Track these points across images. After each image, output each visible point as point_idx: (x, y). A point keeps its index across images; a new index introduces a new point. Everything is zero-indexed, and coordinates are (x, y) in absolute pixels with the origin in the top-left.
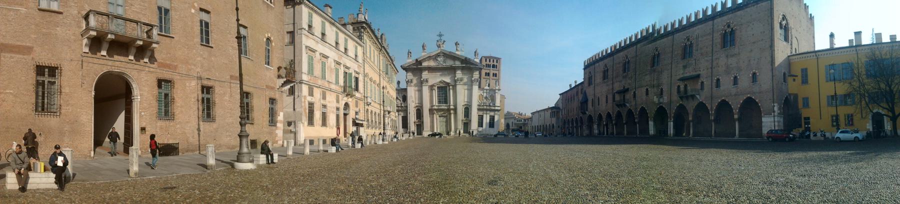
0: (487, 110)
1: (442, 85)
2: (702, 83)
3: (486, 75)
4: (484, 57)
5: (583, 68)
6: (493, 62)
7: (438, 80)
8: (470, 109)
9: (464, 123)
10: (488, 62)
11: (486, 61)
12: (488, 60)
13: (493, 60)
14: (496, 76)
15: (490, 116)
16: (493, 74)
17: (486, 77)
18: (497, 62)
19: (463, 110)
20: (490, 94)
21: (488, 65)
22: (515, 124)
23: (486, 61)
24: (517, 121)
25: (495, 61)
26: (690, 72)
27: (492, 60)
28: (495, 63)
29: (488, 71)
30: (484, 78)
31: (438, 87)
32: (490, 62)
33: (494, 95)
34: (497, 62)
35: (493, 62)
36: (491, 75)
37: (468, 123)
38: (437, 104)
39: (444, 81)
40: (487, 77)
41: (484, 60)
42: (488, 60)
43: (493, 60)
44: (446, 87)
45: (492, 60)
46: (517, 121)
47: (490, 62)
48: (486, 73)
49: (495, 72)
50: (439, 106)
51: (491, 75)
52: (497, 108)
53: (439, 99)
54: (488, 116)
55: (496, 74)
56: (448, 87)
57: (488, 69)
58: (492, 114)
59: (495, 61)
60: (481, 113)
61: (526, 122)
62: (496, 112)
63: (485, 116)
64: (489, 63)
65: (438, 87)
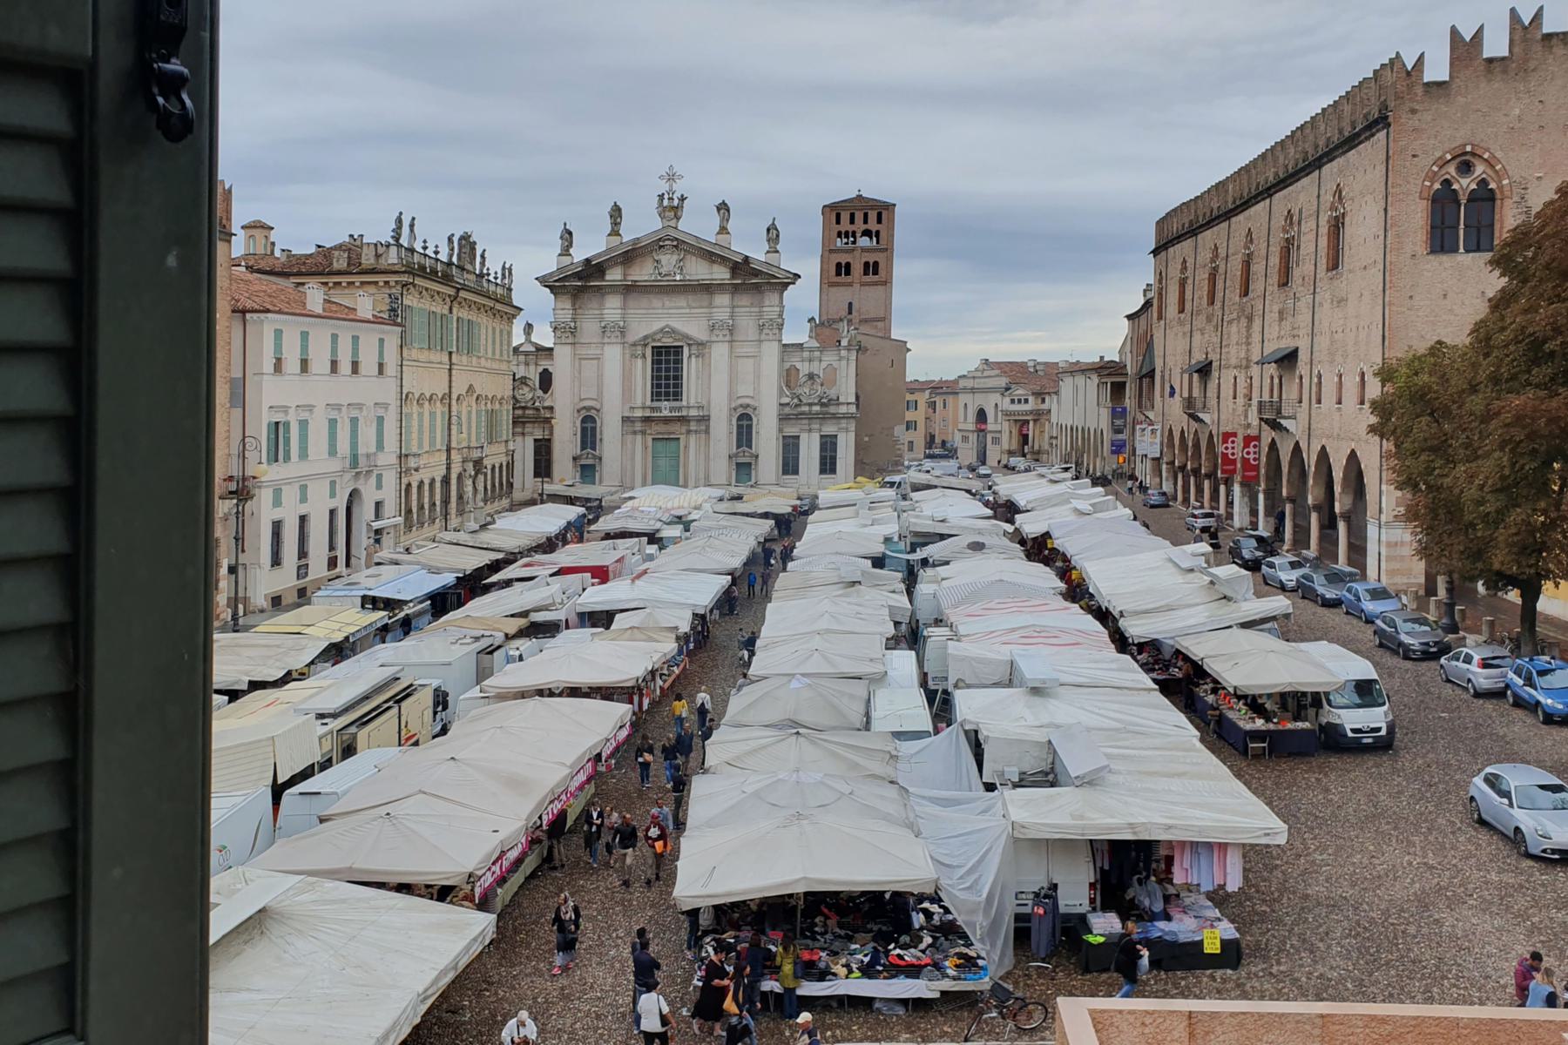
0: (811, 417)
1: (668, 341)
2: (1301, 377)
3: (838, 274)
5: (1153, 247)
6: (866, 222)
7: (657, 326)
8: (755, 419)
9: (737, 464)
10: (845, 225)
11: (838, 222)
12: (845, 217)
13: (866, 215)
14: (876, 272)
15: (822, 436)
16: (867, 264)
17: (838, 279)
18: (879, 221)
19: (734, 422)
20: (824, 365)
22: (1007, 414)
23: (838, 222)
24: (1013, 401)
25: (873, 216)
26: (1287, 344)
27: (859, 216)
28: (873, 225)
29: (844, 259)
31: (653, 347)
32: (852, 221)
33: (835, 364)
34: (879, 221)
35: (866, 222)
36: (857, 269)
37: (750, 464)
38: (648, 403)
39: (674, 331)
40: (843, 278)
42: (845, 217)
43: (866, 215)
44: (682, 347)
45: (859, 216)
46: (1013, 401)
47: (852, 221)
48: (839, 265)
49: (871, 258)
50: (653, 409)
51: (857, 269)
52: (843, 409)
54: (816, 438)
55: (876, 264)
56: (686, 350)
57: (847, 251)
58: (829, 429)
59: (873, 216)
60: (791, 430)
61: (1045, 406)
62: (844, 423)
63: (804, 437)
64: (850, 228)
65: (653, 347)
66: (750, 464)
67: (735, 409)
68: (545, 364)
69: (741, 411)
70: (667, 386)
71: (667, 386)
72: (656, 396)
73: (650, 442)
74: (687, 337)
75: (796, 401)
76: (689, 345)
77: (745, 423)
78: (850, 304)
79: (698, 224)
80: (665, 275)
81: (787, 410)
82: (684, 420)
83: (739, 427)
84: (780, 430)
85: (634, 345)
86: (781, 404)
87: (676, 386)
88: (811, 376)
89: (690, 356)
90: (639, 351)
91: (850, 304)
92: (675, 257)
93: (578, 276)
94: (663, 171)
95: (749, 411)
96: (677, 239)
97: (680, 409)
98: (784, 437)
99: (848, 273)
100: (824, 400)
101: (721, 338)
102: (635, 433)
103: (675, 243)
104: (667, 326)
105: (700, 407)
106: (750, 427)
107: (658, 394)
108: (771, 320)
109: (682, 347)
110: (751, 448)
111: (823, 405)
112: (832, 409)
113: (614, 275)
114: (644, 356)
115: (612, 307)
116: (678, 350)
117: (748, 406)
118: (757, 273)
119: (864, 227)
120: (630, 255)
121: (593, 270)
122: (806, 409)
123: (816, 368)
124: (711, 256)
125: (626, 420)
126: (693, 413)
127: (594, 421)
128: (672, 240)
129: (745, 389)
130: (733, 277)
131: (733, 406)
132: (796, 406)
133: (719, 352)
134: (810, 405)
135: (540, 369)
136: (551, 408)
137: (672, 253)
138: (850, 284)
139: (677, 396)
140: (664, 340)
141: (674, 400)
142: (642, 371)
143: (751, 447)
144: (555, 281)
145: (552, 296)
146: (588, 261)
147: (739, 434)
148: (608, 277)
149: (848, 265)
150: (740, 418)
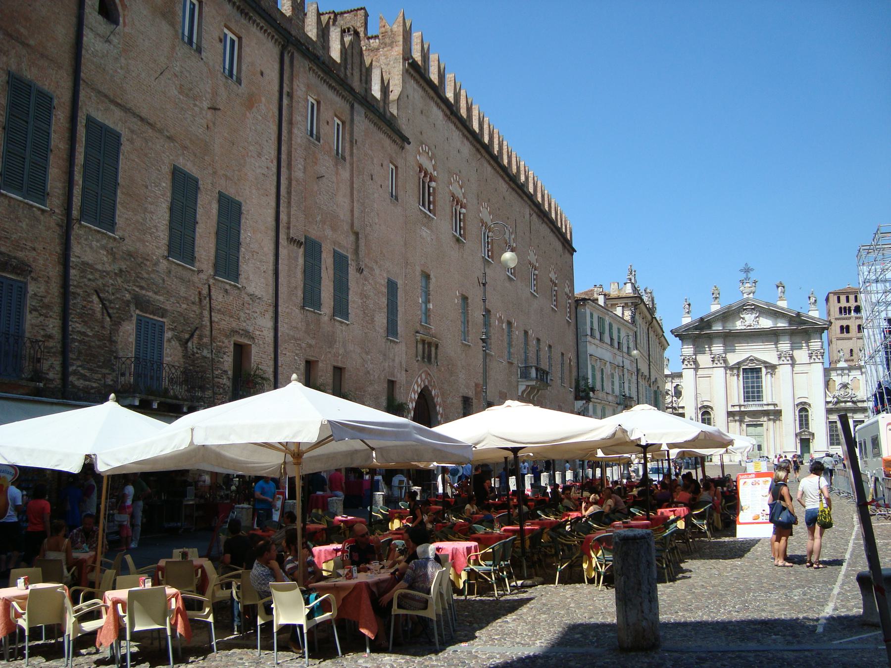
3: (842, 332)
4: (835, 293)
8: (810, 413)
10: (843, 304)
11: (839, 301)
12: (843, 298)
15: (854, 421)
20: (851, 378)
21: (845, 308)
23: (839, 301)
27: (852, 297)
29: (845, 323)
30: (838, 339)
32: (848, 301)
37: (809, 439)
40: (845, 335)
41: (833, 299)
42: (843, 298)
44: (761, 368)
45: (852, 297)
47: (848, 301)
48: (842, 327)
53: (748, 392)
56: (764, 370)
57: (846, 319)
64: (847, 305)
66: (809, 439)
67: (797, 405)
68: (677, 381)
69: (800, 407)
70: (753, 392)
71: (753, 392)
72: (747, 398)
73: (744, 426)
74: (765, 362)
75: (835, 399)
76: (766, 367)
77: (803, 413)
78: (851, 350)
79: (765, 295)
80: (748, 326)
81: (830, 406)
82: (766, 413)
83: (800, 416)
84: (828, 418)
85: (732, 369)
86: (827, 403)
87: (758, 392)
88: (845, 386)
89: (766, 374)
90: (735, 372)
91: (851, 350)
92: (754, 315)
93: (696, 328)
94: (742, 266)
95: (807, 407)
96: (754, 305)
97: (762, 405)
98: (830, 422)
99: (848, 332)
100: (854, 399)
101: (786, 362)
102: (735, 421)
103: (753, 307)
104: (751, 356)
105: (775, 405)
106: (807, 416)
107: (748, 397)
108: (816, 350)
109: (761, 368)
110: (808, 429)
111: (853, 402)
112: (860, 405)
113: (718, 327)
114: (738, 376)
115: (718, 348)
116: (759, 370)
117: (805, 403)
118: (805, 322)
119: (855, 304)
120: (728, 315)
121: (704, 324)
122: (843, 405)
123: (845, 379)
124: (776, 314)
125: (730, 414)
126: (771, 408)
127: (708, 413)
128: (751, 305)
129: (802, 394)
130: (790, 324)
131: (796, 403)
132: (837, 403)
133: (784, 371)
134: (846, 402)
135: (674, 385)
136: (683, 408)
137: (751, 314)
138: (850, 339)
139: (759, 398)
140: (750, 365)
141: (758, 401)
142: (736, 384)
143: (808, 428)
144: (683, 331)
145: (680, 341)
146: (702, 319)
147: (801, 421)
148: (714, 328)
149: (848, 327)
150: (800, 411)
